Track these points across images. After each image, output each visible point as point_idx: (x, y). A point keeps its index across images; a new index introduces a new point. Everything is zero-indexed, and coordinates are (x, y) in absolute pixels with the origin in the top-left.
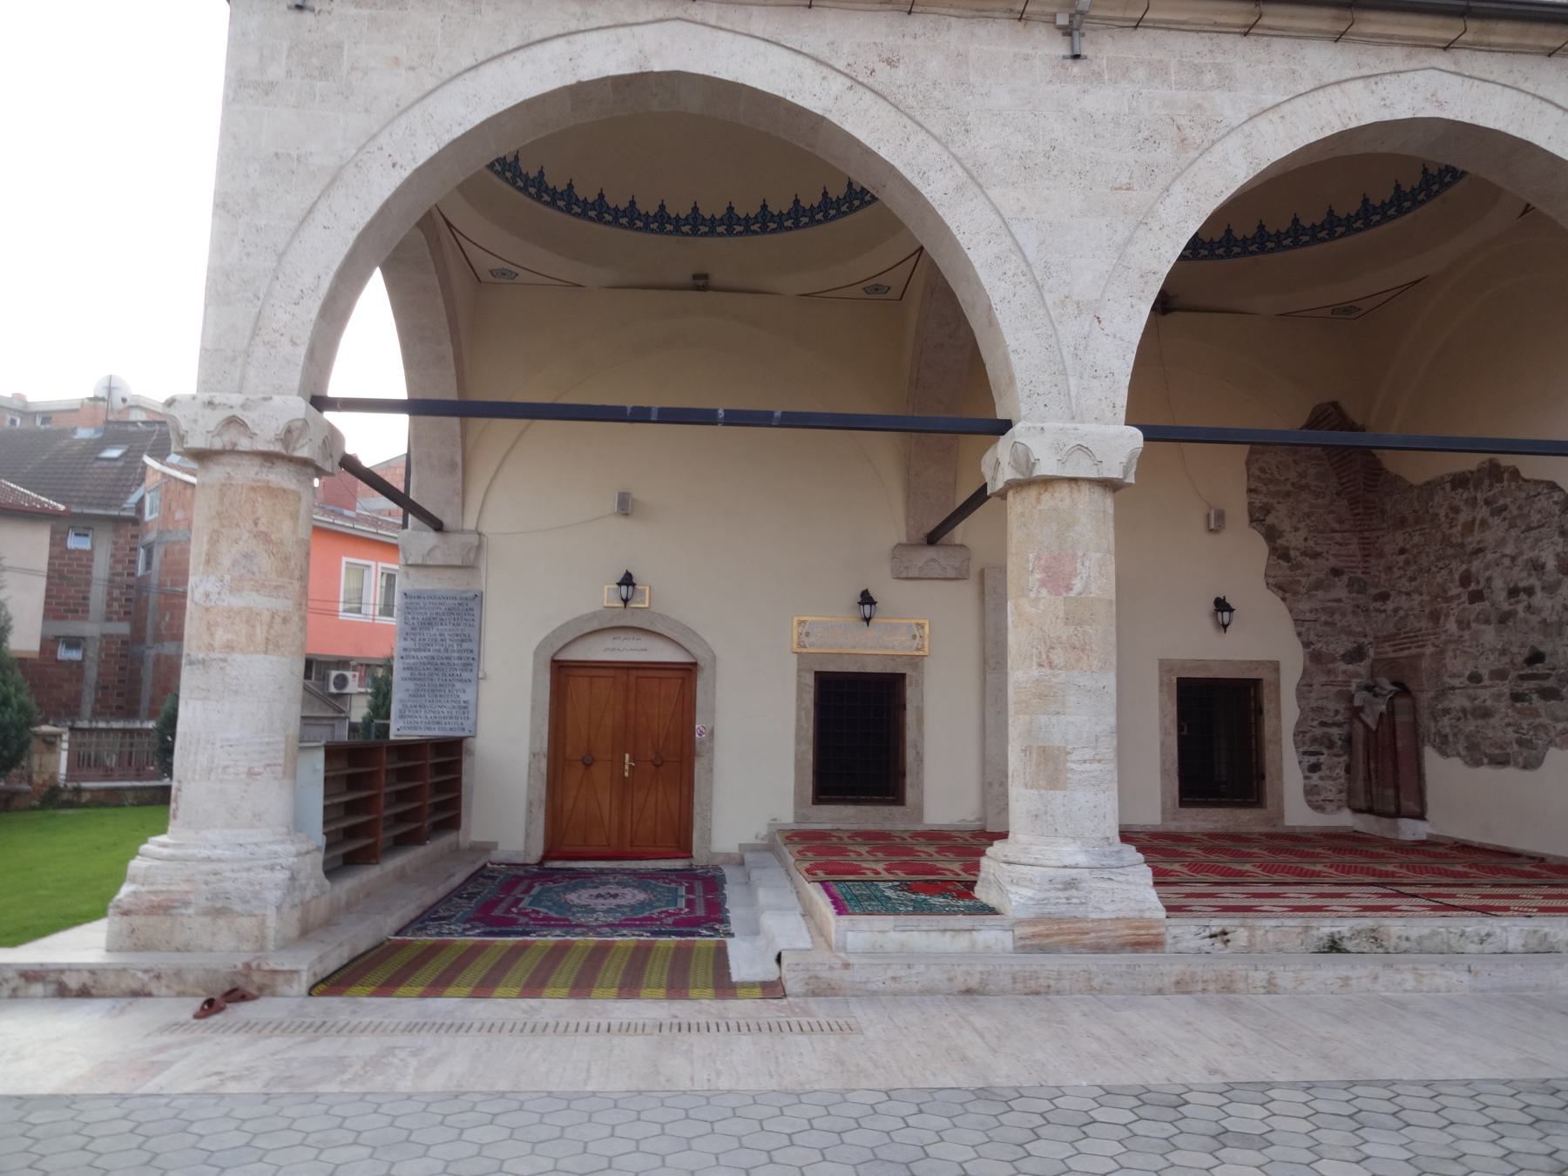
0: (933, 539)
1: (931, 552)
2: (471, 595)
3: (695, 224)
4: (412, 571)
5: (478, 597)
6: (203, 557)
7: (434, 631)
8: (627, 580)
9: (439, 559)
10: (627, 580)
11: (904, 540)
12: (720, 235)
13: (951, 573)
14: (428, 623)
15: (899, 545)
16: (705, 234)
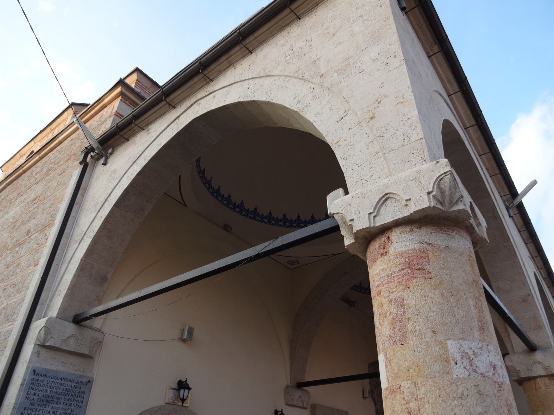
0: (301, 385)
1: (299, 393)
2: (85, 380)
3: (227, 202)
4: (43, 351)
5: (90, 382)
6: (475, 323)
7: (49, 409)
8: (183, 385)
9: (72, 346)
10: (183, 385)
11: (289, 384)
12: (236, 212)
13: (305, 406)
14: (46, 401)
15: (287, 387)
16: (230, 208)
